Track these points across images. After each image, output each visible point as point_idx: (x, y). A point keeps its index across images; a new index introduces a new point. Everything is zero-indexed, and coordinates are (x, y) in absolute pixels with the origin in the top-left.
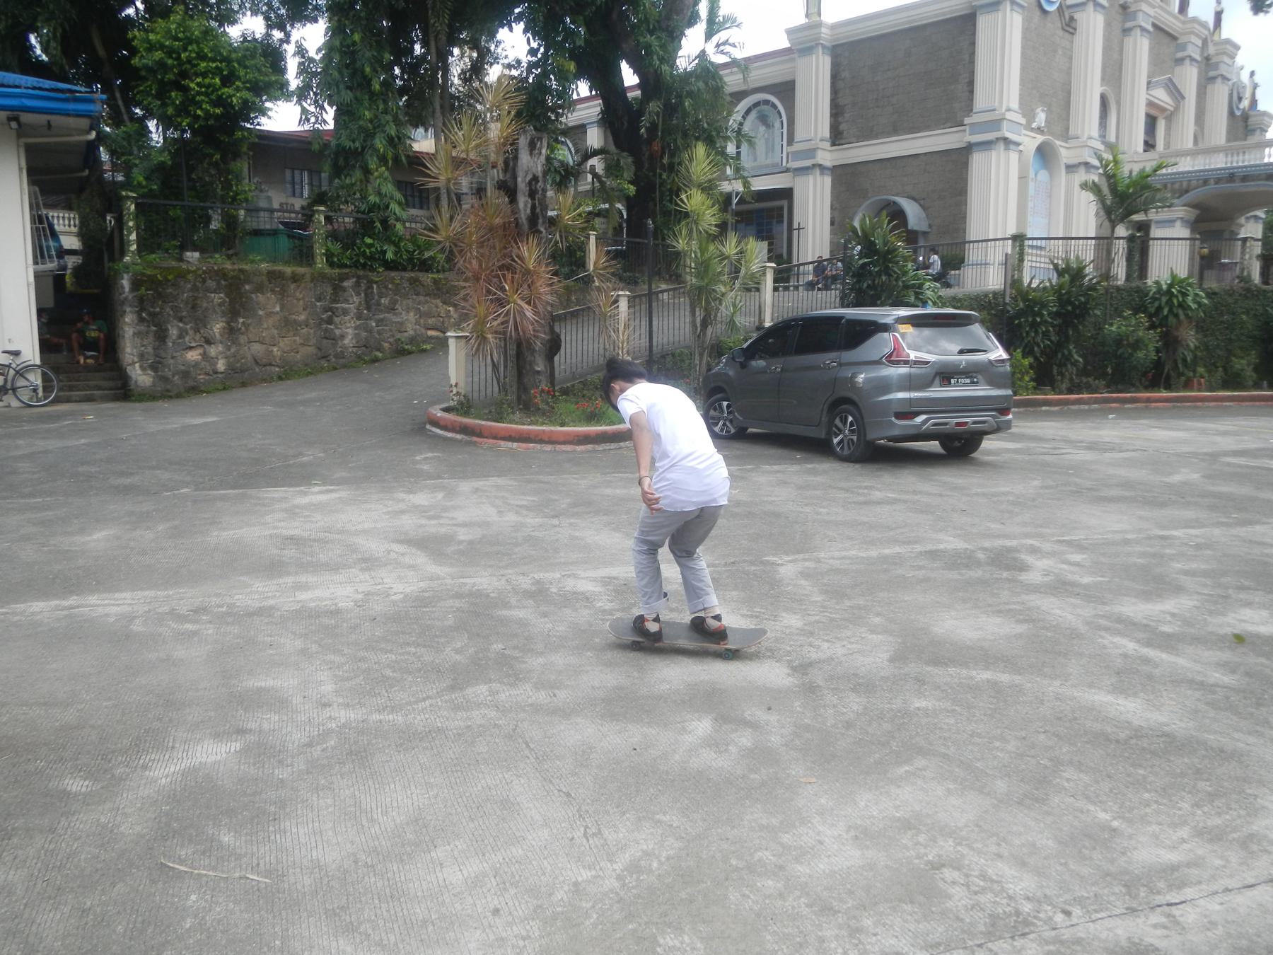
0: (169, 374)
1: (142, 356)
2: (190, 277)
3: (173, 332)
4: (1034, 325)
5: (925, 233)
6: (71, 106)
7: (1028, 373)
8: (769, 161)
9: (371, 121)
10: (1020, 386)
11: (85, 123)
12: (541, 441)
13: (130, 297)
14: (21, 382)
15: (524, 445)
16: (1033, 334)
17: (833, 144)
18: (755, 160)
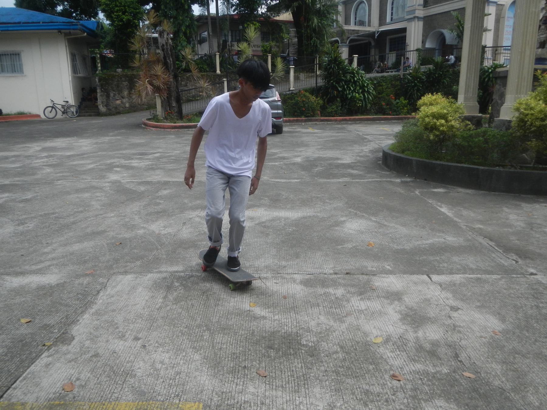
0: (111, 108)
1: (102, 102)
2: (116, 77)
3: (112, 95)
4: (414, 87)
5: (456, 45)
6: (72, 27)
7: (406, 107)
8: (403, 16)
9: (182, 20)
10: (402, 112)
11: (79, 31)
12: (161, 128)
13: (98, 84)
14: (69, 110)
15: (156, 129)
16: (412, 91)
17: (424, 7)
18: (398, 15)
